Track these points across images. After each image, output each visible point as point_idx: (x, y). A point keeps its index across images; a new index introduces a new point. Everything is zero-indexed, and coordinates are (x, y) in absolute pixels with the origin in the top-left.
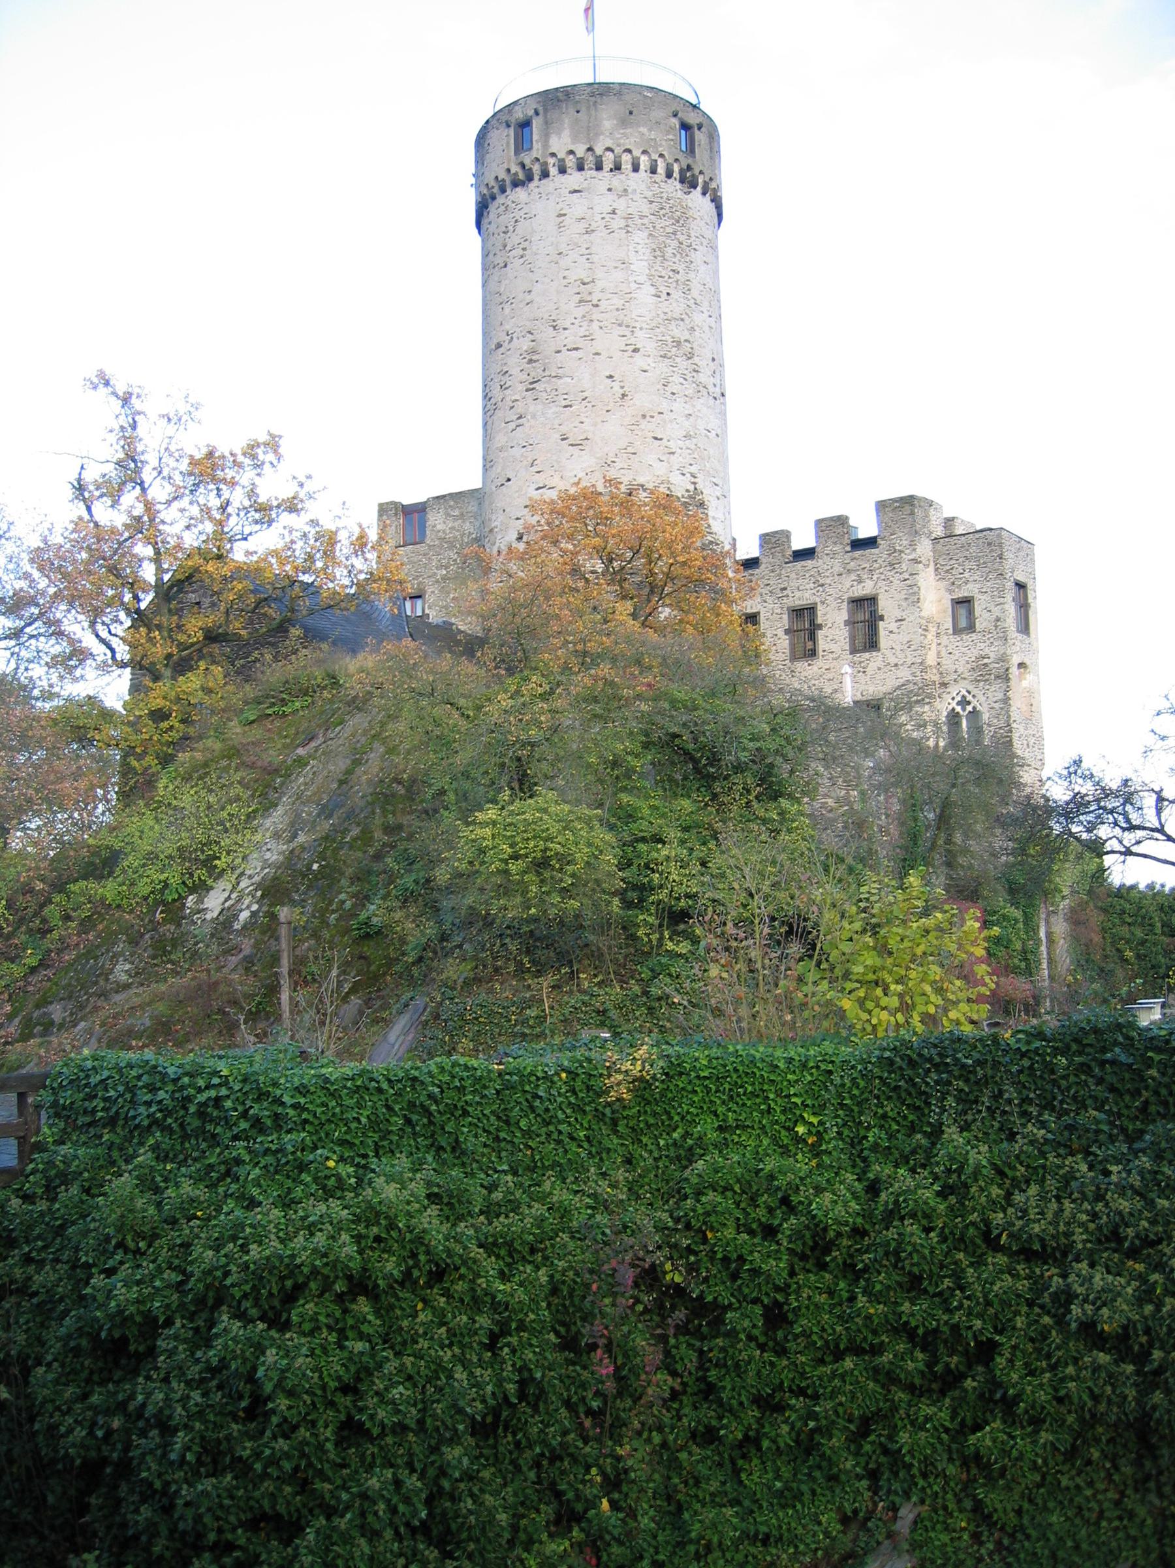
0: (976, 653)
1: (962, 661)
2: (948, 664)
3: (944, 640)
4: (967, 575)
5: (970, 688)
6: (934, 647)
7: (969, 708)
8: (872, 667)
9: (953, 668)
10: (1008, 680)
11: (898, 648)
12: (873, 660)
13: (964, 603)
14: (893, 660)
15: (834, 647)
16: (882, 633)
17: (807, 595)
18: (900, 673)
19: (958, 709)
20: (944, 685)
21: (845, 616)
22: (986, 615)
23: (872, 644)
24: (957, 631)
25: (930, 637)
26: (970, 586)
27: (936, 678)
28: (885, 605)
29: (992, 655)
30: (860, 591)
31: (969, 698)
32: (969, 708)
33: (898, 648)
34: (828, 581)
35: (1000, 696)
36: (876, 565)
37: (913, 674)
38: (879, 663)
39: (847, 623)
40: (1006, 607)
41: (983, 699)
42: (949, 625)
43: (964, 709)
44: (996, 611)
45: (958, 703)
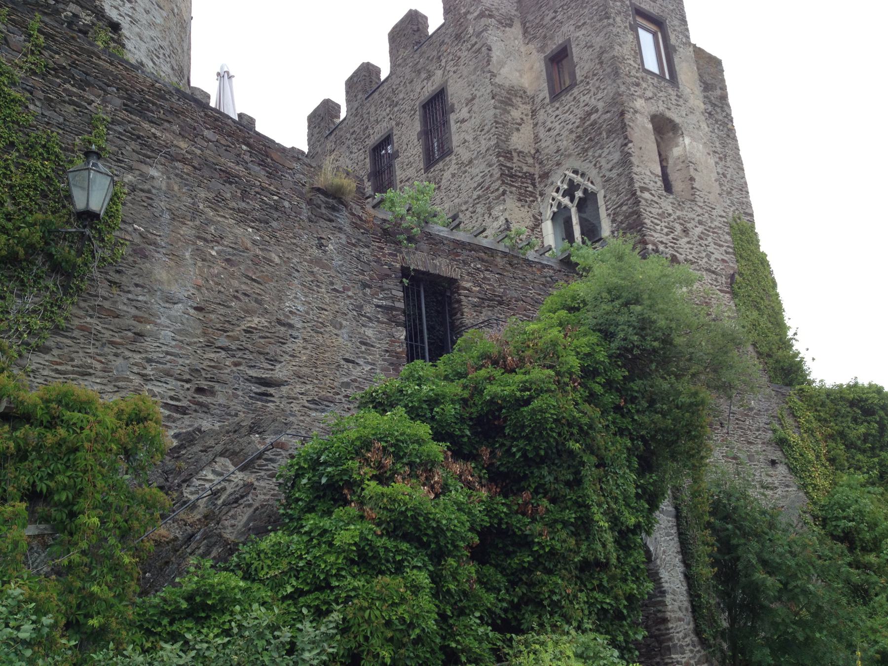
0: (579, 112)
1: (565, 133)
2: (548, 145)
3: (541, 116)
4: (559, 17)
5: (578, 164)
6: (527, 130)
7: (579, 194)
8: (447, 175)
9: (553, 148)
10: (624, 127)
11: (470, 138)
12: (448, 169)
13: (559, 59)
14: (465, 156)
15: (411, 172)
16: (454, 127)
17: (385, 124)
18: (474, 171)
19: (566, 201)
20: (545, 176)
21: (417, 126)
22: (587, 54)
23: (446, 152)
24: (555, 96)
25: (516, 114)
26: (564, 29)
27: (537, 171)
28: (457, 92)
29: (601, 105)
30: (430, 89)
31: (577, 179)
32: (579, 194)
33: (470, 138)
34: (401, 96)
35: (616, 156)
36: (444, 48)
37: (490, 165)
38: (453, 168)
39: (420, 135)
40: (615, 30)
41: (593, 173)
42: (546, 93)
43: (572, 200)
44: (598, 41)
45: (564, 196)
